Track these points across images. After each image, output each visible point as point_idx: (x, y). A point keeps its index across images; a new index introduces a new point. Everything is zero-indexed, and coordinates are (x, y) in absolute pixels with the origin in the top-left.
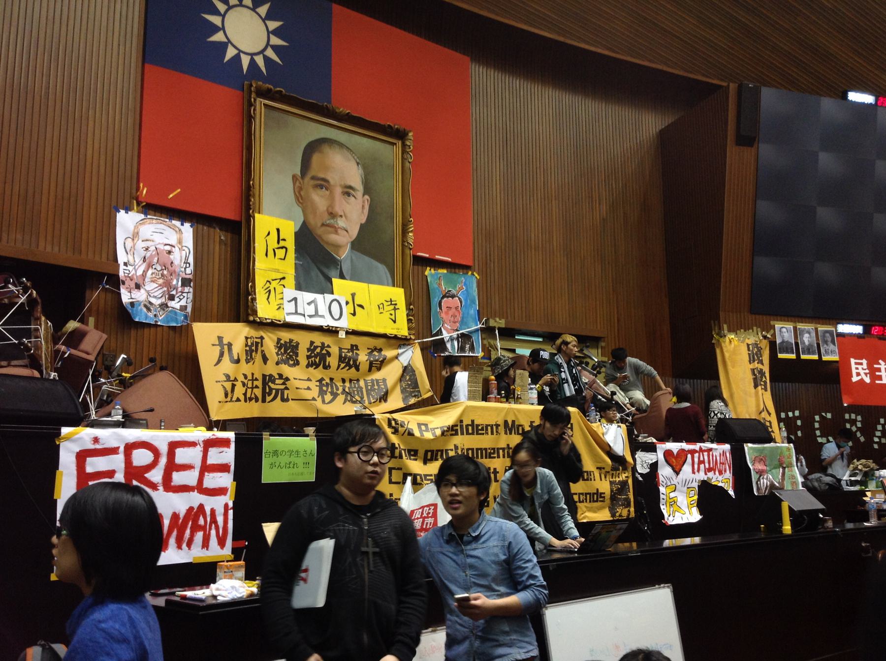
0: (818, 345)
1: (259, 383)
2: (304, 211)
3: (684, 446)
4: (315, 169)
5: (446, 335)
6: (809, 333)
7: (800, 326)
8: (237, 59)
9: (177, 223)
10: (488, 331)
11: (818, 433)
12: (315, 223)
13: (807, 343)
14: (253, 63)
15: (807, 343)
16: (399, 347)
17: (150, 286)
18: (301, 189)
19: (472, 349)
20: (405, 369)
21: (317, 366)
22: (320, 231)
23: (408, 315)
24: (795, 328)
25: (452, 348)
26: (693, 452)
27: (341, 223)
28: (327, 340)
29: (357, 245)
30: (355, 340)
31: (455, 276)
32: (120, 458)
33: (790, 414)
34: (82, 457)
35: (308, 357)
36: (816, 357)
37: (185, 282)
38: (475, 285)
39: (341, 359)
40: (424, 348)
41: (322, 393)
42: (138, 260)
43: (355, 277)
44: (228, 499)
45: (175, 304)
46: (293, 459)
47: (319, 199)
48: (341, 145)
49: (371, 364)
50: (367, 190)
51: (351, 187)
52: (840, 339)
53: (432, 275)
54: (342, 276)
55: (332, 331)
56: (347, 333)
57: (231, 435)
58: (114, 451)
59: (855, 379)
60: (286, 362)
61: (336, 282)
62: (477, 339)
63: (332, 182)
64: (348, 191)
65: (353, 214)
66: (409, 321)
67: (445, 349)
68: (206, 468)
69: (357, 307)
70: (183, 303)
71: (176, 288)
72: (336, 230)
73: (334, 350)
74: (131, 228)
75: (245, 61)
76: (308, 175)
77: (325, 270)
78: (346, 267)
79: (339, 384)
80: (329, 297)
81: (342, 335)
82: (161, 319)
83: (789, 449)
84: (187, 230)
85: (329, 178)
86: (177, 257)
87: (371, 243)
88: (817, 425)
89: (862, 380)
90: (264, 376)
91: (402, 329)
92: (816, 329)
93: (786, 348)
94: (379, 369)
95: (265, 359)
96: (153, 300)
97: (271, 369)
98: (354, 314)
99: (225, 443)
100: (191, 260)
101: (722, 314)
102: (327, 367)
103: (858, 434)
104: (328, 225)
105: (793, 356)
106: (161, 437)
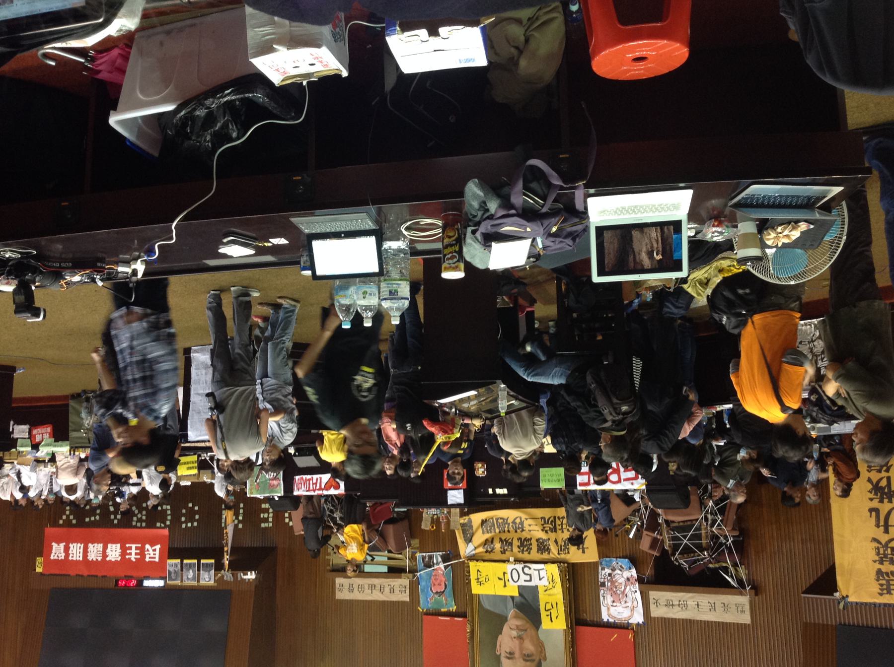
0: (182, 570)
1: (558, 527)
3: (325, 493)
5: (442, 566)
6: (188, 579)
7: (195, 583)
9: (611, 620)
10: (413, 571)
11: (169, 512)
13: (191, 571)
15: (191, 571)
16: (474, 555)
17: (622, 580)
18: (541, 652)
19: (424, 558)
20: (470, 541)
21: (525, 539)
22: (528, 625)
24: (198, 581)
25: (437, 556)
26: (320, 489)
27: (514, 633)
28: (520, 556)
30: (503, 557)
31: (436, 607)
32: (623, 477)
33: (189, 525)
35: (531, 544)
36: (185, 561)
37: (603, 584)
38: (421, 602)
39: (511, 544)
40: (458, 556)
41: (522, 523)
42: (630, 595)
43: (504, 598)
45: (608, 571)
46: (550, 478)
47: (529, 647)
49: (492, 542)
50: (498, 658)
51: (509, 658)
52: (163, 575)
53: (452, 606)
54: (512, 598)
55: (517, 561)
56: (508, 561)
57: (579, 488)
58: (625, 480)
59: (158, 547)
60: (544, 541)
61: (516, 594)
62: (420, 564)
64: (511, 656)
66: (469, 572)
67: (442, 557)
69: (503, 579)
70: (603, 572)
71: (608, 581)
72: (517, 626)
73: (515, 549)
74: (635, 614)
77: (523, 600)
78: (510, 604)
79: (511, 529)
80: (519, 583)
81: (512, 559)
82: (614, 562)
83: (251, 493)
84: (605, 617)
86: (609, 599)
87: (496, 622)
88: (169, 518)
89: (152, 546)
90: (556, 531)
91: (473, 566)
92: (182, 581)
93: (207, 567)
94: (487, 540)
95: (556, 541)
96: (619, 572)
97: (552, 536)
98: (504, 573)
99: (581, 484)
100: (601, 599)
101: (253, 588)
102: (519, 539)
103: (136, 512)
105: (203, 561)
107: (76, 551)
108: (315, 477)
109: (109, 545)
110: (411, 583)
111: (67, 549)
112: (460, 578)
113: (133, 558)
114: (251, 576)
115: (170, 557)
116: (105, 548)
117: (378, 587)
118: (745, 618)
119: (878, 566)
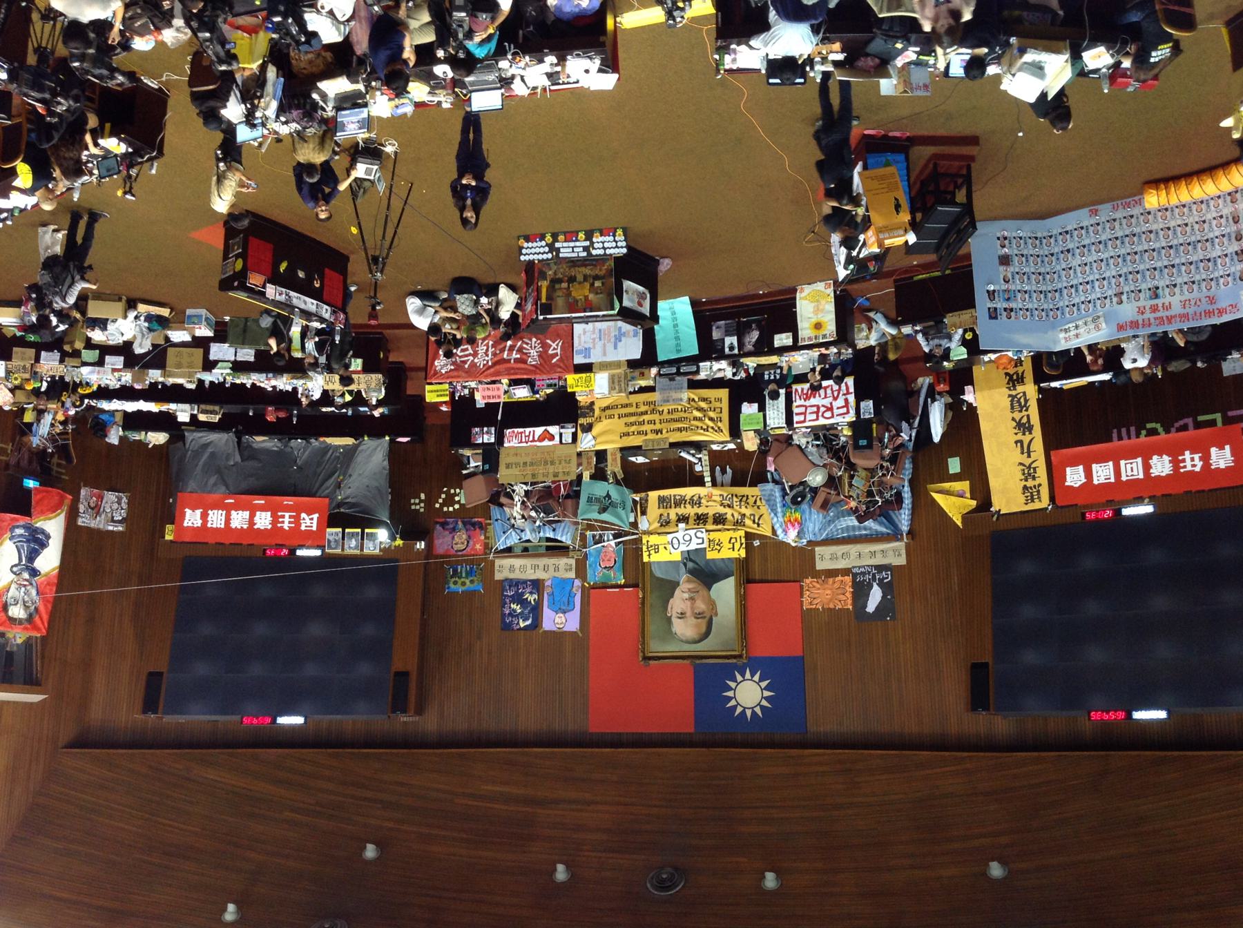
0: (343, 538)
7: (358, 552)
8: (752, 676)
14: (743, 676)
24: (362, 549)
26: (534, 441)
27: (686, 596)
29: (675, 585)
34: (848, 412)
36: (347, 530)
44: (795, 404)
47: (701, 606)
48: (688, 642)
50: (669, 620)
59: (316, 516)
64: (682, 615)
65: (679, 602)
68: (805, 414)
75: (748, 675)
85: (695, 620)
106: (822, 422)
107: (216, 519)
108: (528, 430)
109: (258, 513)
110: (577, 561)
111: (204, 516)
112: (632, 552)
113: (286, 526)
114: (421, 545)
115: (329, 526)
116: (252, 516)
117: (541, 567)
118: (902, 561)
119: (1024, 483)
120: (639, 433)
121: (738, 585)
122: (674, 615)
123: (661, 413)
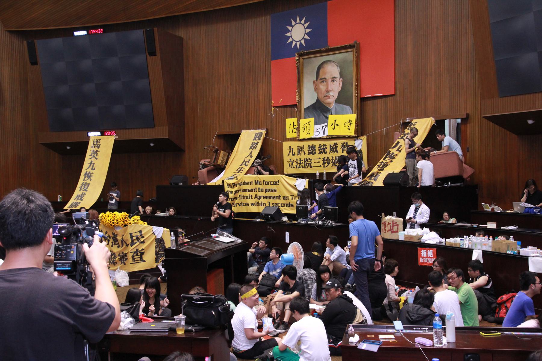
1: (303, 162)
2: (318, 94)
4: (321, 76)
12: (321, 96)
16: (355, 140)
18: (316, 85)
21: (322, 153)
22: (322, 100)
23: (355, 126)
43: (336, 113)
47: (323, 87)
50: (341, 76)
51: (335, 78)
54: (331, 114)
60: (311, 153)
63: (327, 78)
64: (333, 79)
65: (335, 88)
66: (356, 128)
72: (329, 98)
76: (319, 78)
77: (325, 114)
91: (352, 133)
104: (326, 96)
120: (267, 183)
121: (300, 102)
122: (338, 79)
123: (256, 197)
